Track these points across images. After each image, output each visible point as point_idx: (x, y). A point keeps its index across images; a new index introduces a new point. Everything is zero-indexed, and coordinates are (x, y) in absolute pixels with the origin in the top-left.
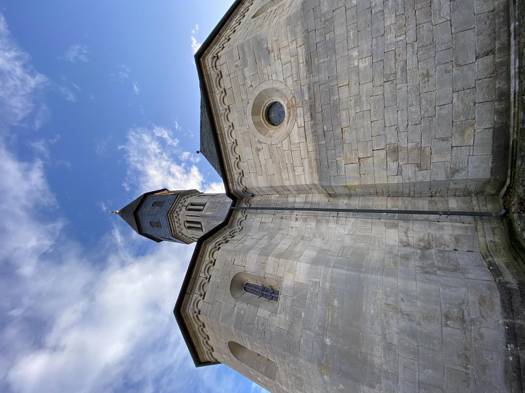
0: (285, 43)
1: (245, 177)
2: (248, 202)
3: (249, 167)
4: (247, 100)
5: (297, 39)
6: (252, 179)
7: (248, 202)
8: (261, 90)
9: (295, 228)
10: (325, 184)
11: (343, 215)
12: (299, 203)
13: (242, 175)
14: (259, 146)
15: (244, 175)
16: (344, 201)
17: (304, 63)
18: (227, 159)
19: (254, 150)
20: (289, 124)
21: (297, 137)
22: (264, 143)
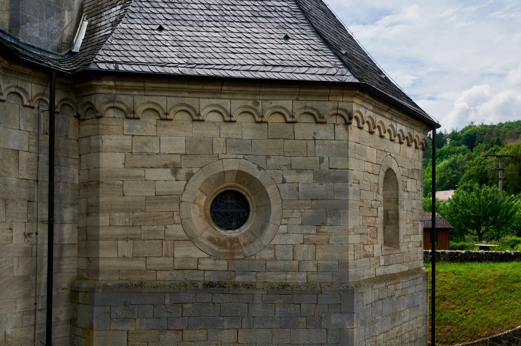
0: (320, 254)
1: (125, 120)
2: (64, 105)
3: (145, 138)
4: (264, 167)
5: (318, 274)
6: (119, 137)
7: (64, 105)
8: (272, 200)
9: (10, 235)
10: (98, 296)
11: (38, 319)
12: (61, 233)
13: (129, 115)
14: (182, 173)
15: (128, 120)
16: (63, 315)
17: (284, 281)
18: (169, 90)
19: (177, 159)
20: (207, 243)
21: (184, 254)
22: (185, 186)
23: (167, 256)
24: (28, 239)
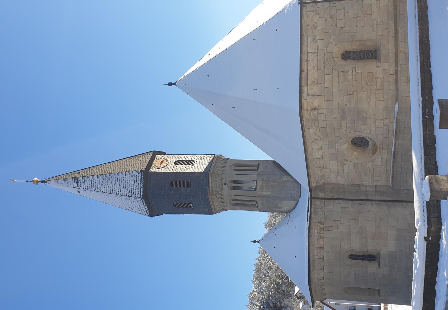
14: (344, 162)
20: (375, 156)
23: (381, 167)
24: (373, 205)
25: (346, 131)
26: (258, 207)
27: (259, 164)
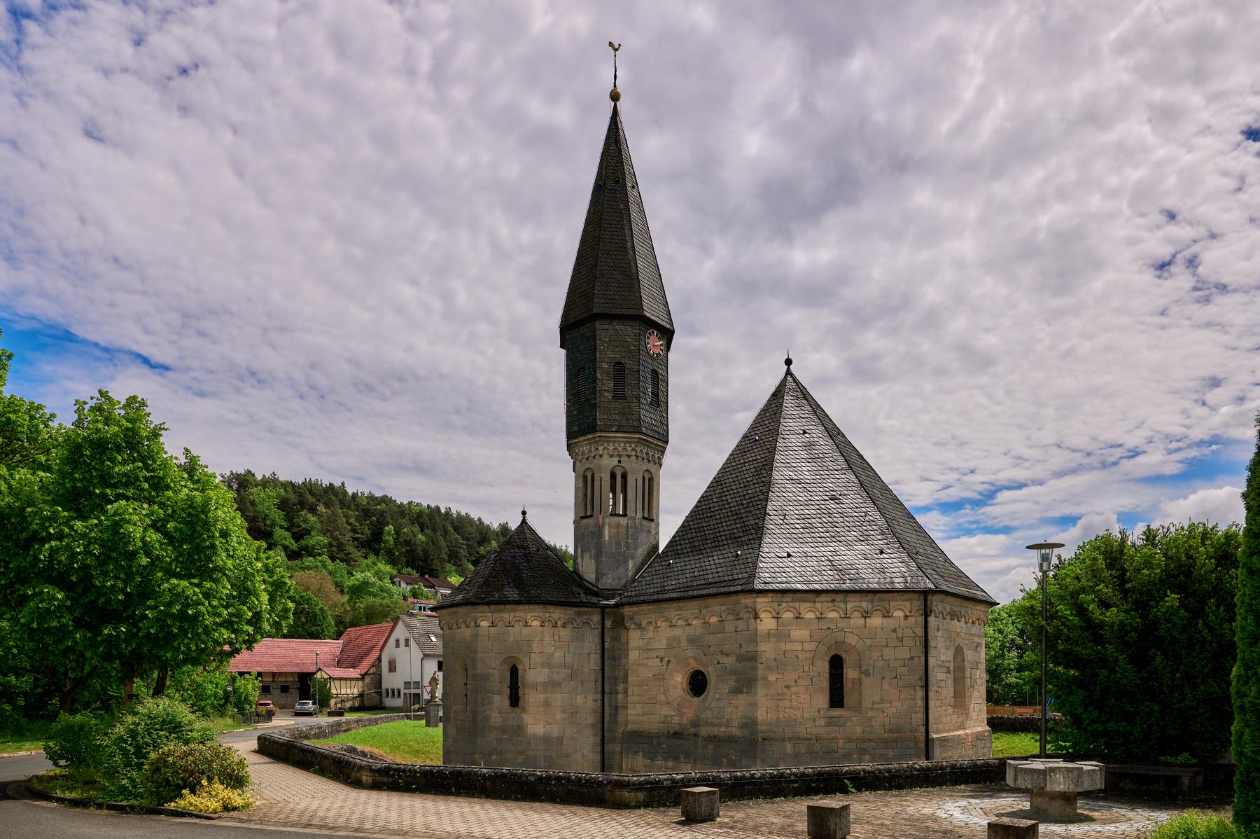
14: (665, 662)
25: (718, 663)
26: (582, 518)
27: (652, 520)
